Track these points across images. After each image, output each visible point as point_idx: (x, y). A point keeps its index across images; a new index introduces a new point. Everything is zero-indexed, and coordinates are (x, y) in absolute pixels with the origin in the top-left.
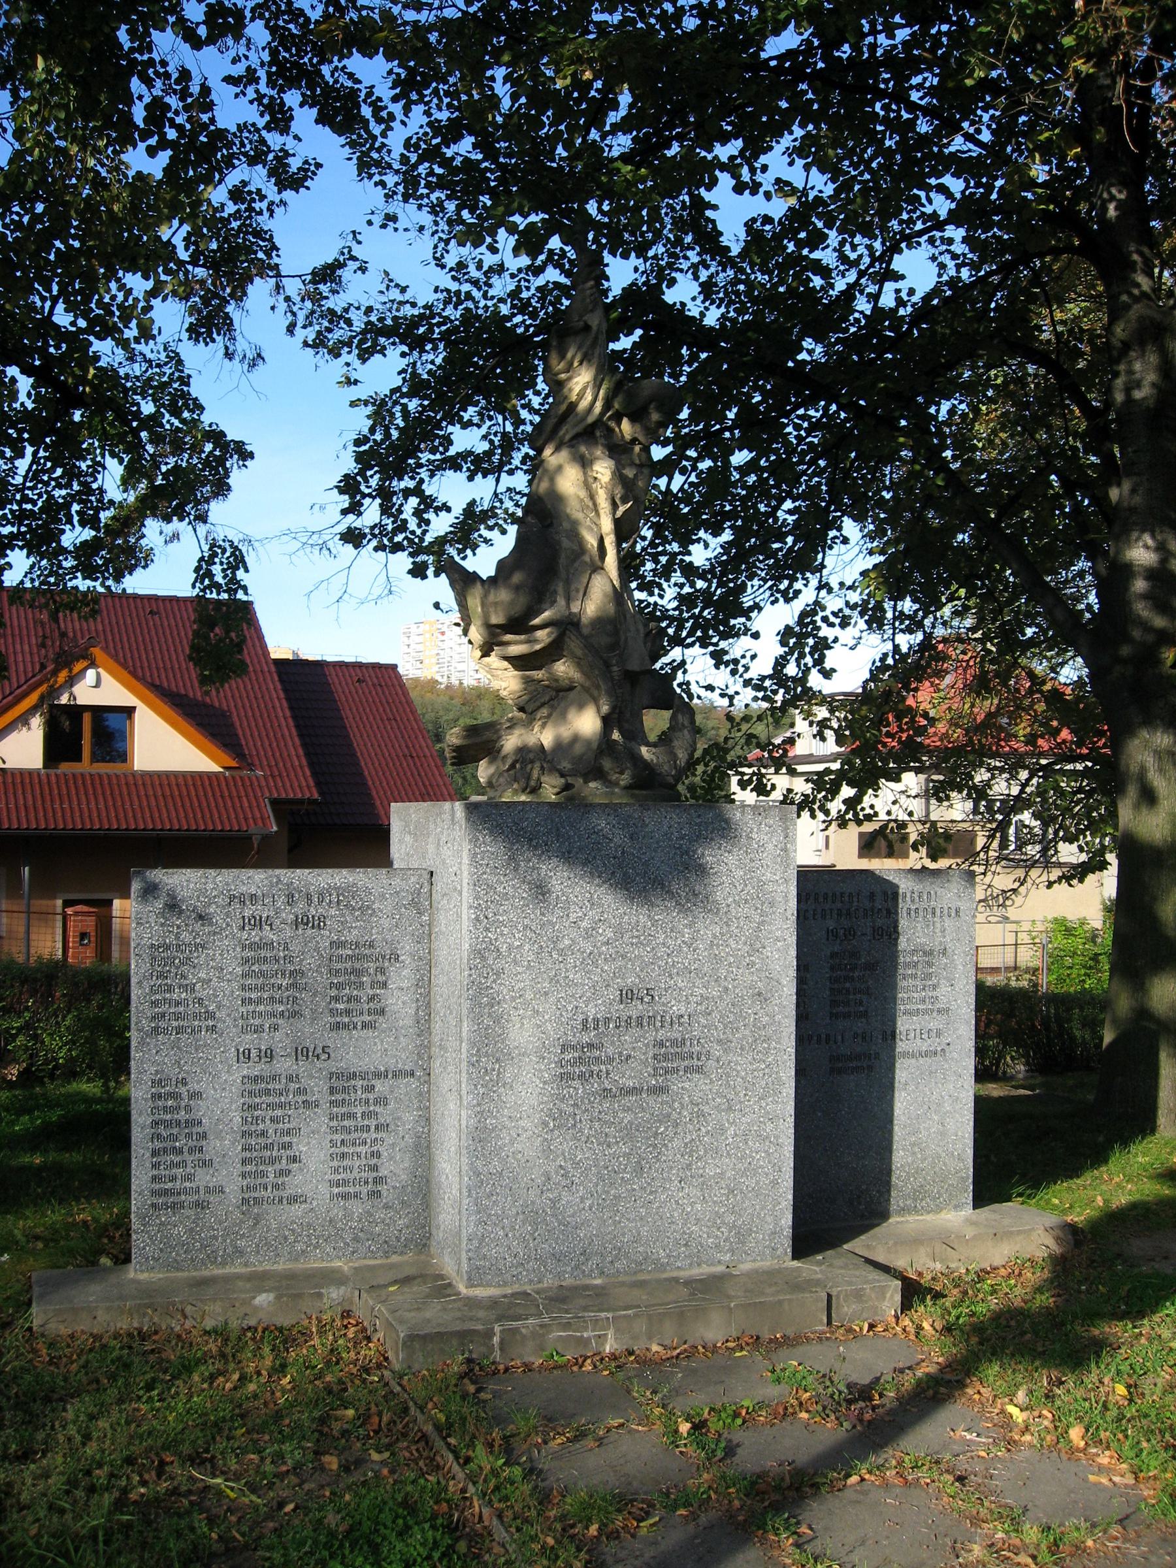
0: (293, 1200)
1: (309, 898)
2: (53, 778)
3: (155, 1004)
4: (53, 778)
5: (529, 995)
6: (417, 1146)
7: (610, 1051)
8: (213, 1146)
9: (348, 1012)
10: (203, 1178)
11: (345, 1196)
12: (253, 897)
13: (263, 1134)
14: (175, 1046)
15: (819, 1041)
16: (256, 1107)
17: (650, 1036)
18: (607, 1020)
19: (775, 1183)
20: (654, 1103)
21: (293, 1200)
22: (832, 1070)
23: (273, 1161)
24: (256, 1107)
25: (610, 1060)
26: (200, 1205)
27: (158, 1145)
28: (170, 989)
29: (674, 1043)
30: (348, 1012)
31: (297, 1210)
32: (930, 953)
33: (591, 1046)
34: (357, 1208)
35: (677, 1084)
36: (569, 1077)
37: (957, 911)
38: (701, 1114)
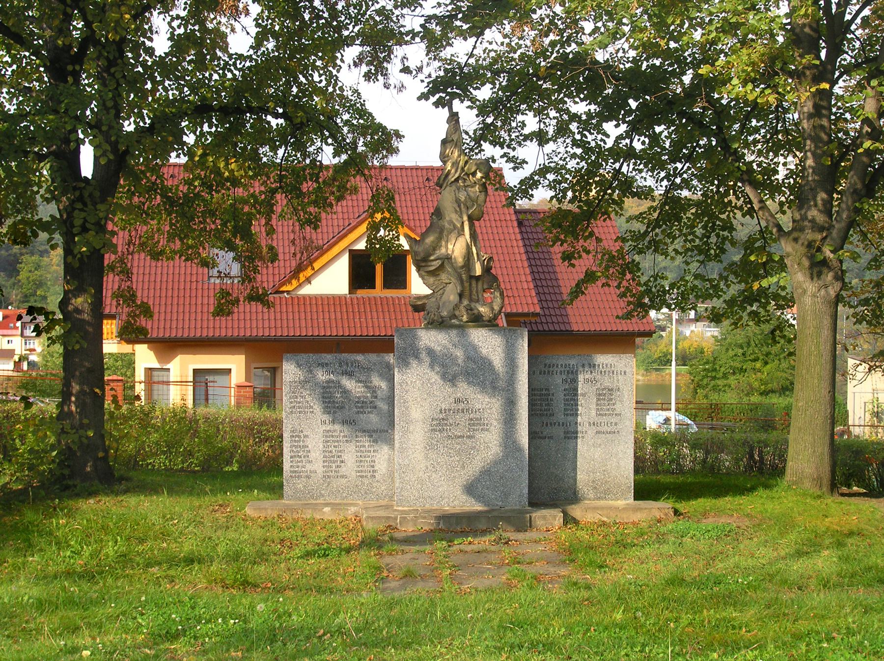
0: (342, 477)
1: (347, 364)
2: (355, 302)
3: (291, 402)
4: (355, 302)
5: (419, 399)
6: (389, 459)
7: (451, 421)
8: (313, 455)
9: (362, 407)
10: (309, 467)
11: (362, 477)
12: (327, 364)
13: (331, 452)
14: (299, 418)
15: (559, 425)
16: (328, 442)
17: (467, 417)
18: (450, 410)
19: (520, 476)
20: (469, 442)
21: (342, 477)
22: (565, 438)
23: (334, 462)
24: (328, 442)
25: (451, 425)
26: (308, 477)
27: (293, 454)
28: (297, 397)
29: (477, 419)
30: (362, 407)
31: (344, 481)
32: (612, 390)
33: (443, 419)
34: (366, 481)
35: (478, 435)
36: (435, 430)
37: (625, 373)
38: (488, 447)
